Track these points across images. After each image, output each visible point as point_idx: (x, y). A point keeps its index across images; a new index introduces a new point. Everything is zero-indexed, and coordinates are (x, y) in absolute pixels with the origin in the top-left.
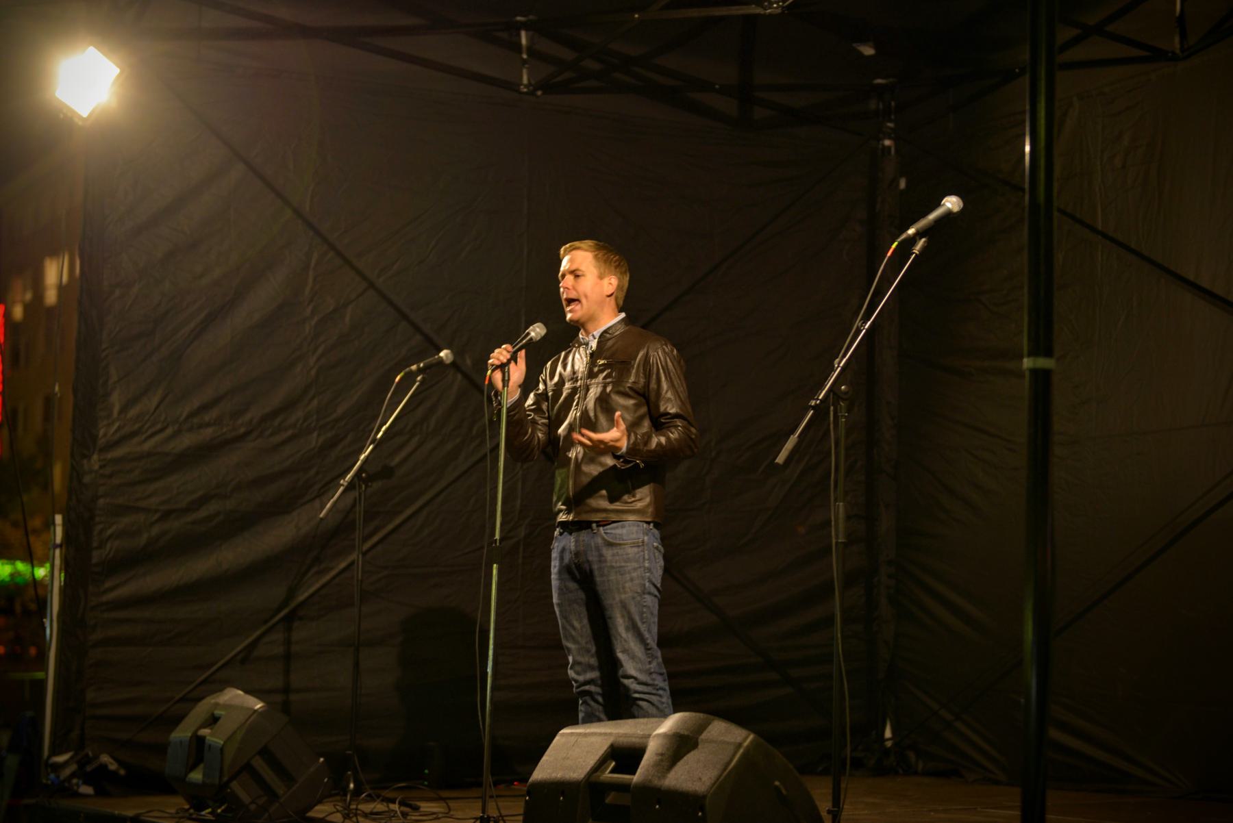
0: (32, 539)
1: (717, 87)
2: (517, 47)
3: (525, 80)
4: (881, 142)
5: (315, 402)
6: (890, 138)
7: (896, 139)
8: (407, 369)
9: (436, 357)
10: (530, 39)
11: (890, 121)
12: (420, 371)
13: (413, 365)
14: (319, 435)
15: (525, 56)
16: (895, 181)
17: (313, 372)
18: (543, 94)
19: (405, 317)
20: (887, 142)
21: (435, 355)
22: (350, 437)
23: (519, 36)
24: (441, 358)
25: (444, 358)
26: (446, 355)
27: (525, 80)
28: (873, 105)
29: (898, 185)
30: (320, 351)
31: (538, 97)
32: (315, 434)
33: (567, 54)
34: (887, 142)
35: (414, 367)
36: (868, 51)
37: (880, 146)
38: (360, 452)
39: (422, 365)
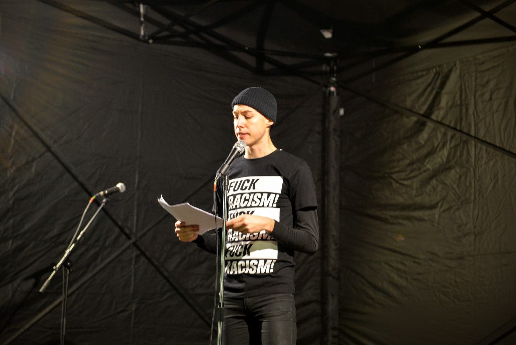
0: (138, 252)
1: (247, 48)
2: (138, 14)
3: (142, 33)
4: (328, 88)
5: (11, 221)
6: (334, 86)
7: (337, 88)
8: (97, 194)
9: (115, 187)
10: (146, 10)
11: (334, 77)
12: (105, 195)
13: (101, 191)
14: (13, 242)
15: (142, 19)
16: (337, 111)
17: (11, 202)
18: (153, 43)
19: (68, 170)
20: (332, 89)
21: (113, 186)
22: (32, 245)
23: (139, 7)
24: (118, 188)
25: (120, 188)
26: (122, 187)
27: (142, 33)
28: (325, 68)
29: (339, 113)
30: (16, 188)
31: (148, 43)
32: (11, 242)
33: (166, 22)
34: (332, 89)
35: (102, 193)
36: (328, 35)
37: (328, 91)
38: (66, 248)
39: (106, 192)
